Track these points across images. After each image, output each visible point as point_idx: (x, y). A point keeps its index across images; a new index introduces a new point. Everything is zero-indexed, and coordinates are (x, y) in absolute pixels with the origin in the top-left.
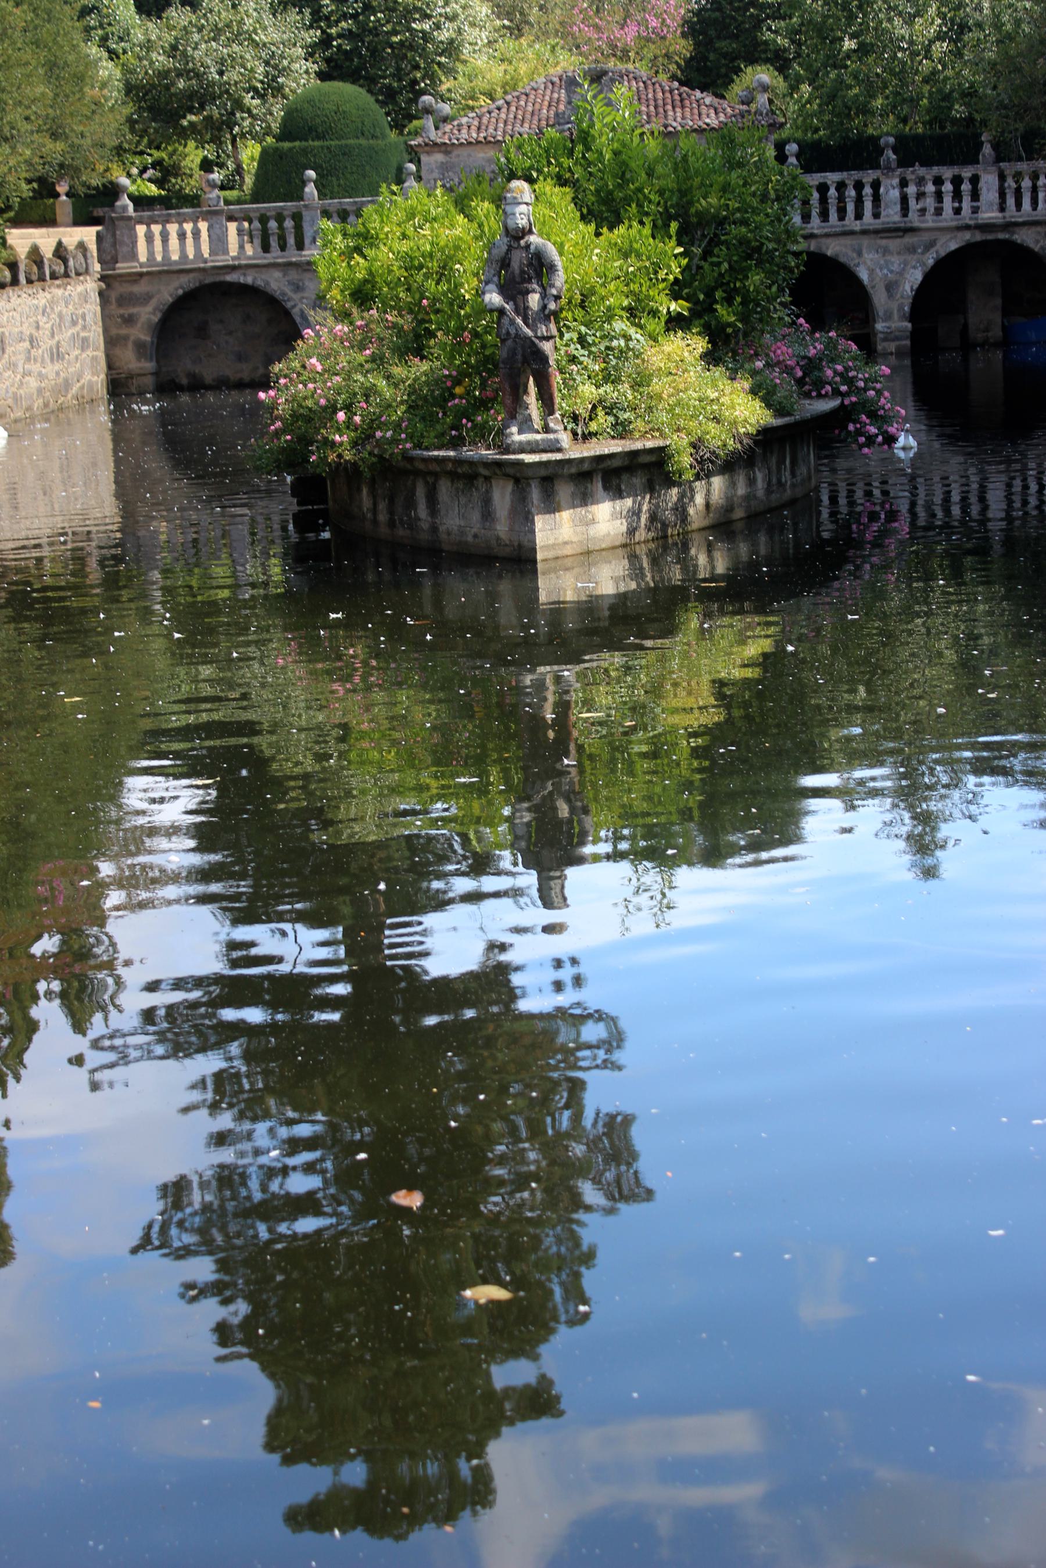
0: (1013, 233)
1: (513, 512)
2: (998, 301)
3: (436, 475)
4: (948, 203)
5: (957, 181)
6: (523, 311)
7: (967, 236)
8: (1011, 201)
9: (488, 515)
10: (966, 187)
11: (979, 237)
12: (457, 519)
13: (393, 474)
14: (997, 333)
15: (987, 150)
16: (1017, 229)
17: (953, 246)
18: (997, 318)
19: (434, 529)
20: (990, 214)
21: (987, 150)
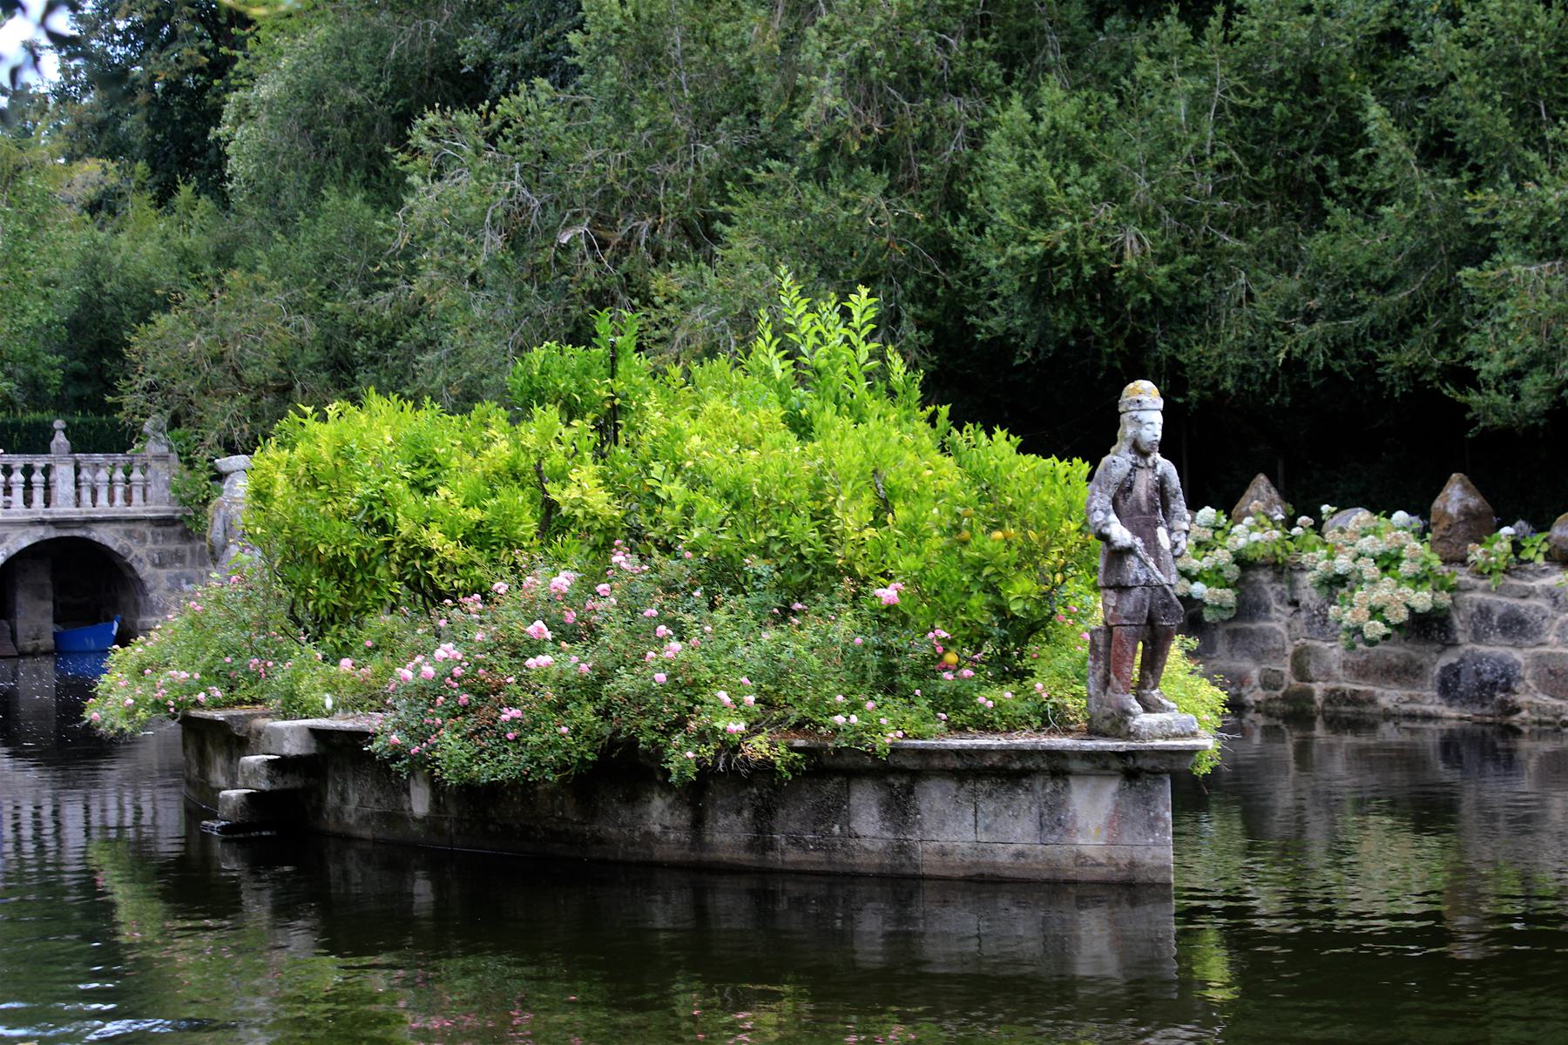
0: (90, 530)
1: (1118, 819)
2: (49, 605)
3: (917, 775)
4: (18, 493)
5: (28, 471)
6: (1153, 546)
7: (41, 533)
8: (86, 495)
9: (1053, 820)
10: (38, 478)
11: (53, 533)
12: (954, 830)
13: (831, 770)
14: (47, 641)
15: (60, 438)
16: (93, 526)
17: (26, 542)
18: (49, 627)
19: (902, 849)
20: (63, 508)
21: (60, 438)
